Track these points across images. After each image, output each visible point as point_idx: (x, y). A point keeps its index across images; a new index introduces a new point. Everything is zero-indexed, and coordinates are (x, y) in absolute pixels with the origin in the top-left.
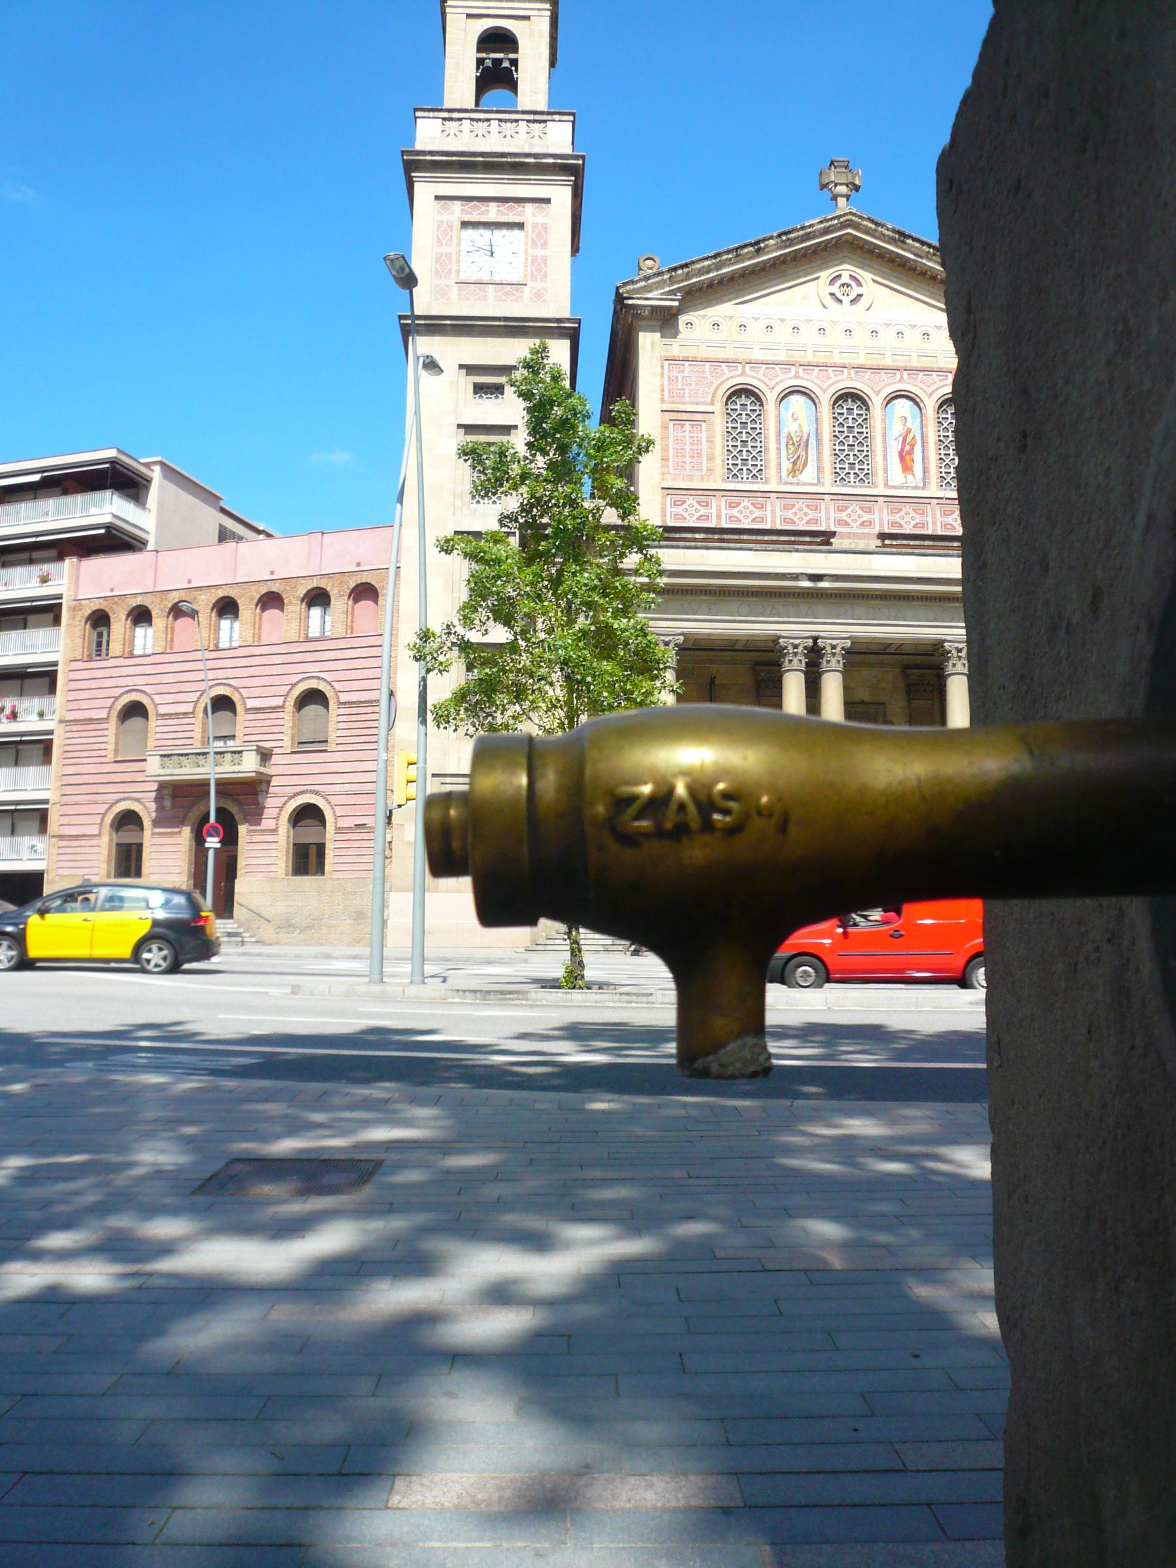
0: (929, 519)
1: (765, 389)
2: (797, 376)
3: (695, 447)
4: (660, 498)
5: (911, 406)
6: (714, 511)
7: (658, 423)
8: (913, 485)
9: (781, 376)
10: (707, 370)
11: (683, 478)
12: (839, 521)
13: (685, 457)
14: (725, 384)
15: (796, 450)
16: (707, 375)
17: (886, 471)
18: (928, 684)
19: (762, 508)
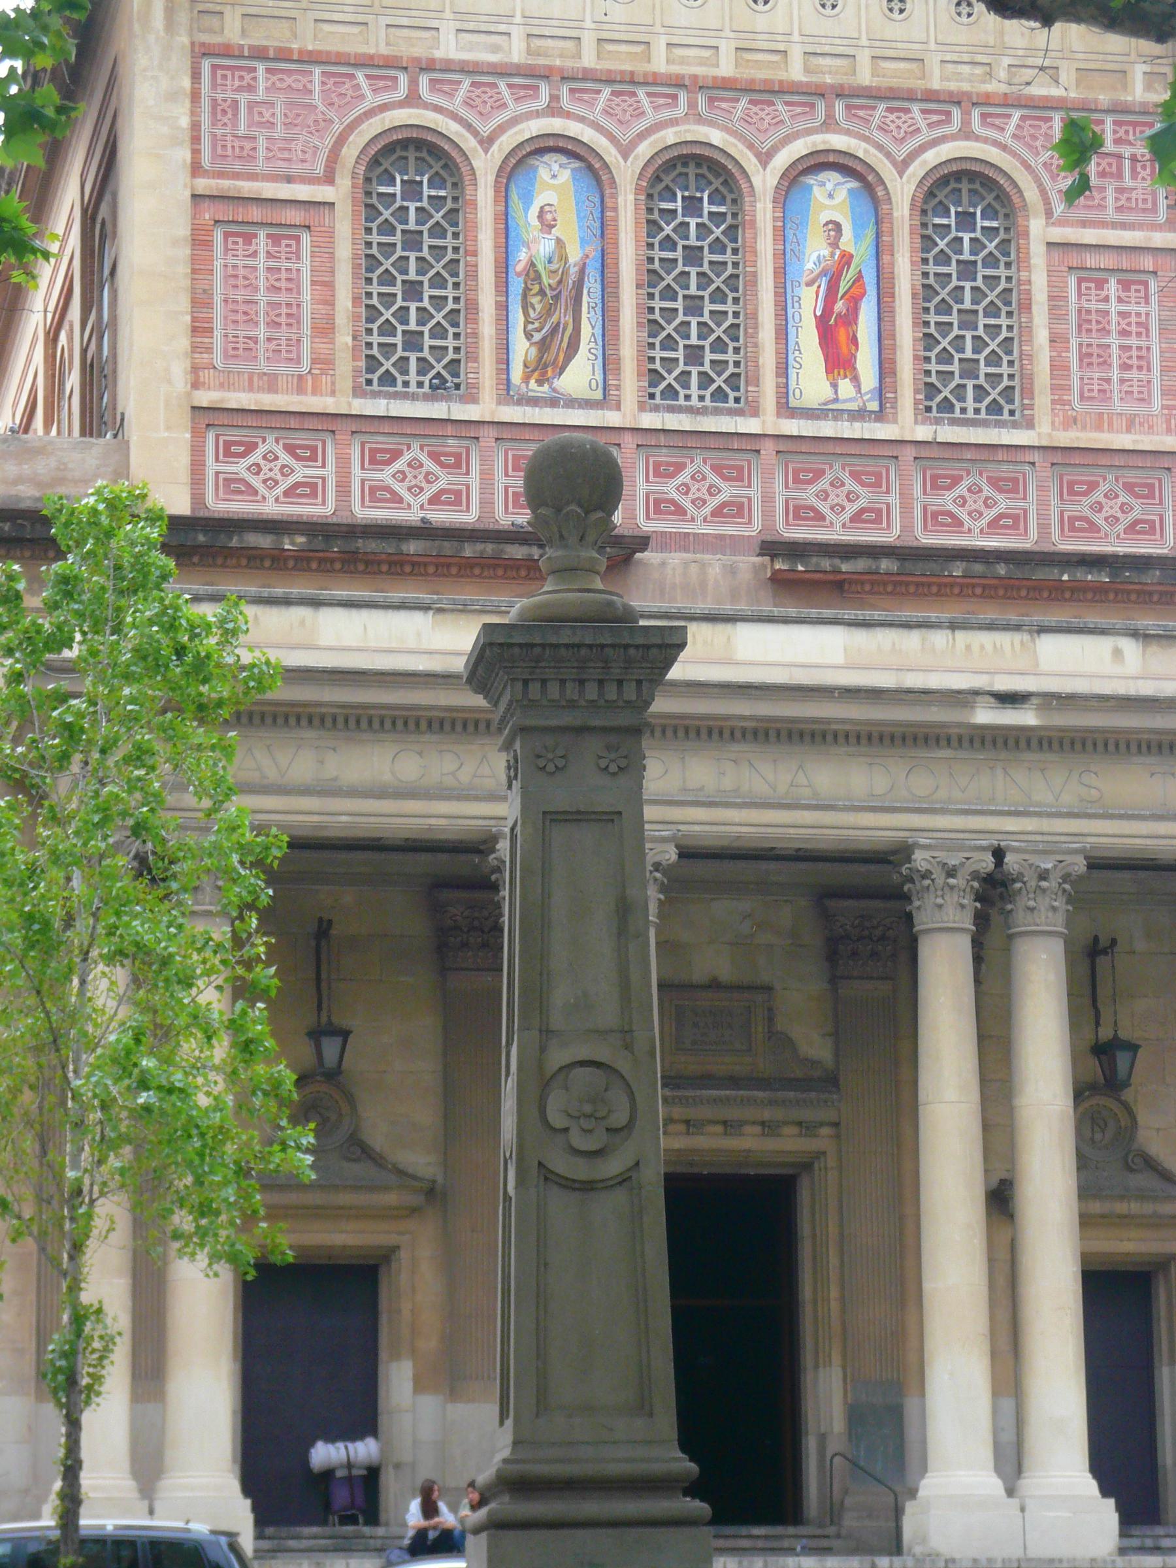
0: (894, 499)
1: (469, 143)
2: (553, 109)
3: (283, 297)
4: (188, 436)
5: (850, 191)
6: (330, 472)
7: (183, 230)
8: (853, 406)
9: (514, 109)
10: (317, 87)
11: (251, 380)
12: (657, 502)
13: (256, 324)
14: (364, 126)
15: (549, 311)
16: (317, 98)
17: (783, 369)
18: (883, 938)
19: (457, 465)
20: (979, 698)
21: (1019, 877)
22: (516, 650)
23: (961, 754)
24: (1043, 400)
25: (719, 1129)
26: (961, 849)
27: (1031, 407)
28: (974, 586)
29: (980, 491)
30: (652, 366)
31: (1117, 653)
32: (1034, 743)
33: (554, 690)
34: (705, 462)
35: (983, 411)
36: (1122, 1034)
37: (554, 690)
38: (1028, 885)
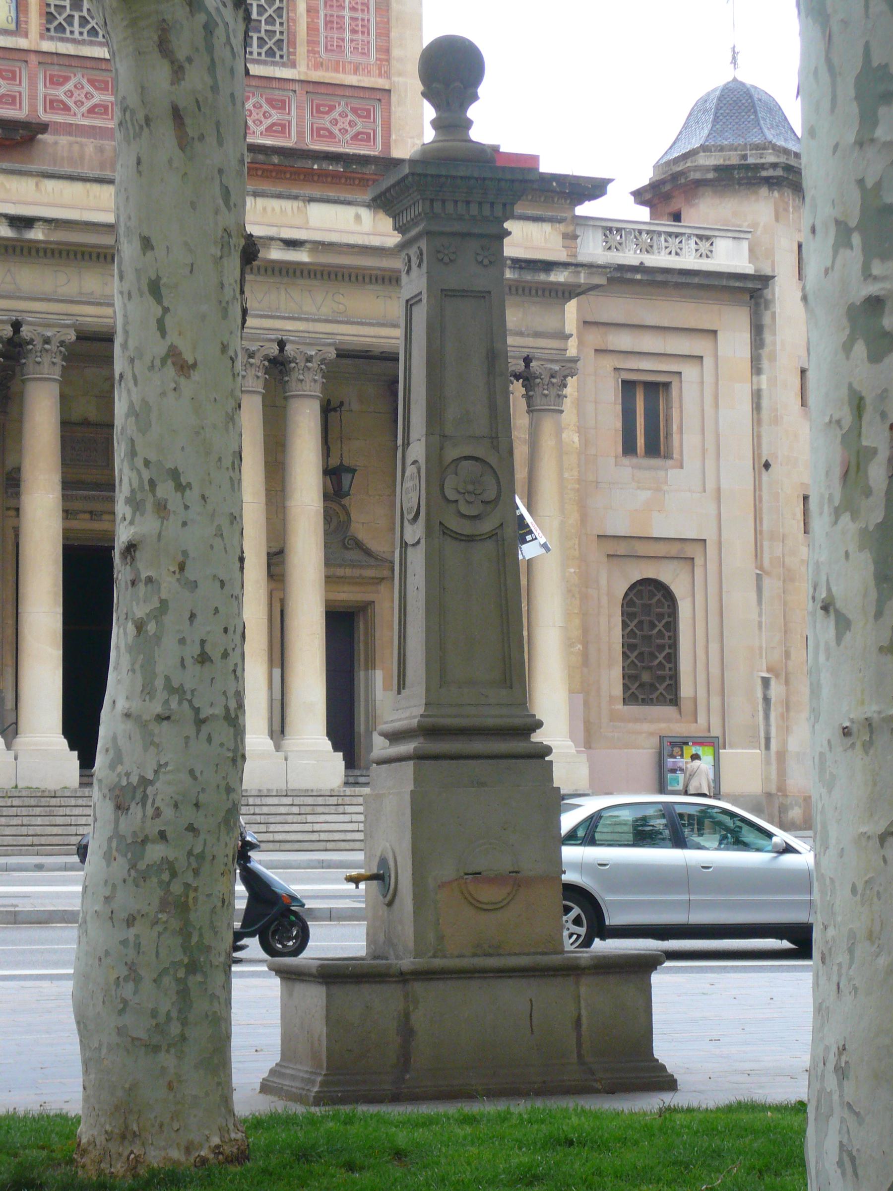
12: (51, 102)
20: (273, 242)
21: (294, 360)
22: (429, 179)
23: (260, 278)
24: (302, 50)
25: (87, 516)
26: (258, 340)
27: (294, 54)
28: (257, 169)
29: (261, 107)
30: (48, 10)
31: (358, 217)
32: (305, 273)
33: (450, 207)
34: (83, 76)
35: (263, 54)
36: (346, 462)
37: (450, 207)
38: (299, 365)
